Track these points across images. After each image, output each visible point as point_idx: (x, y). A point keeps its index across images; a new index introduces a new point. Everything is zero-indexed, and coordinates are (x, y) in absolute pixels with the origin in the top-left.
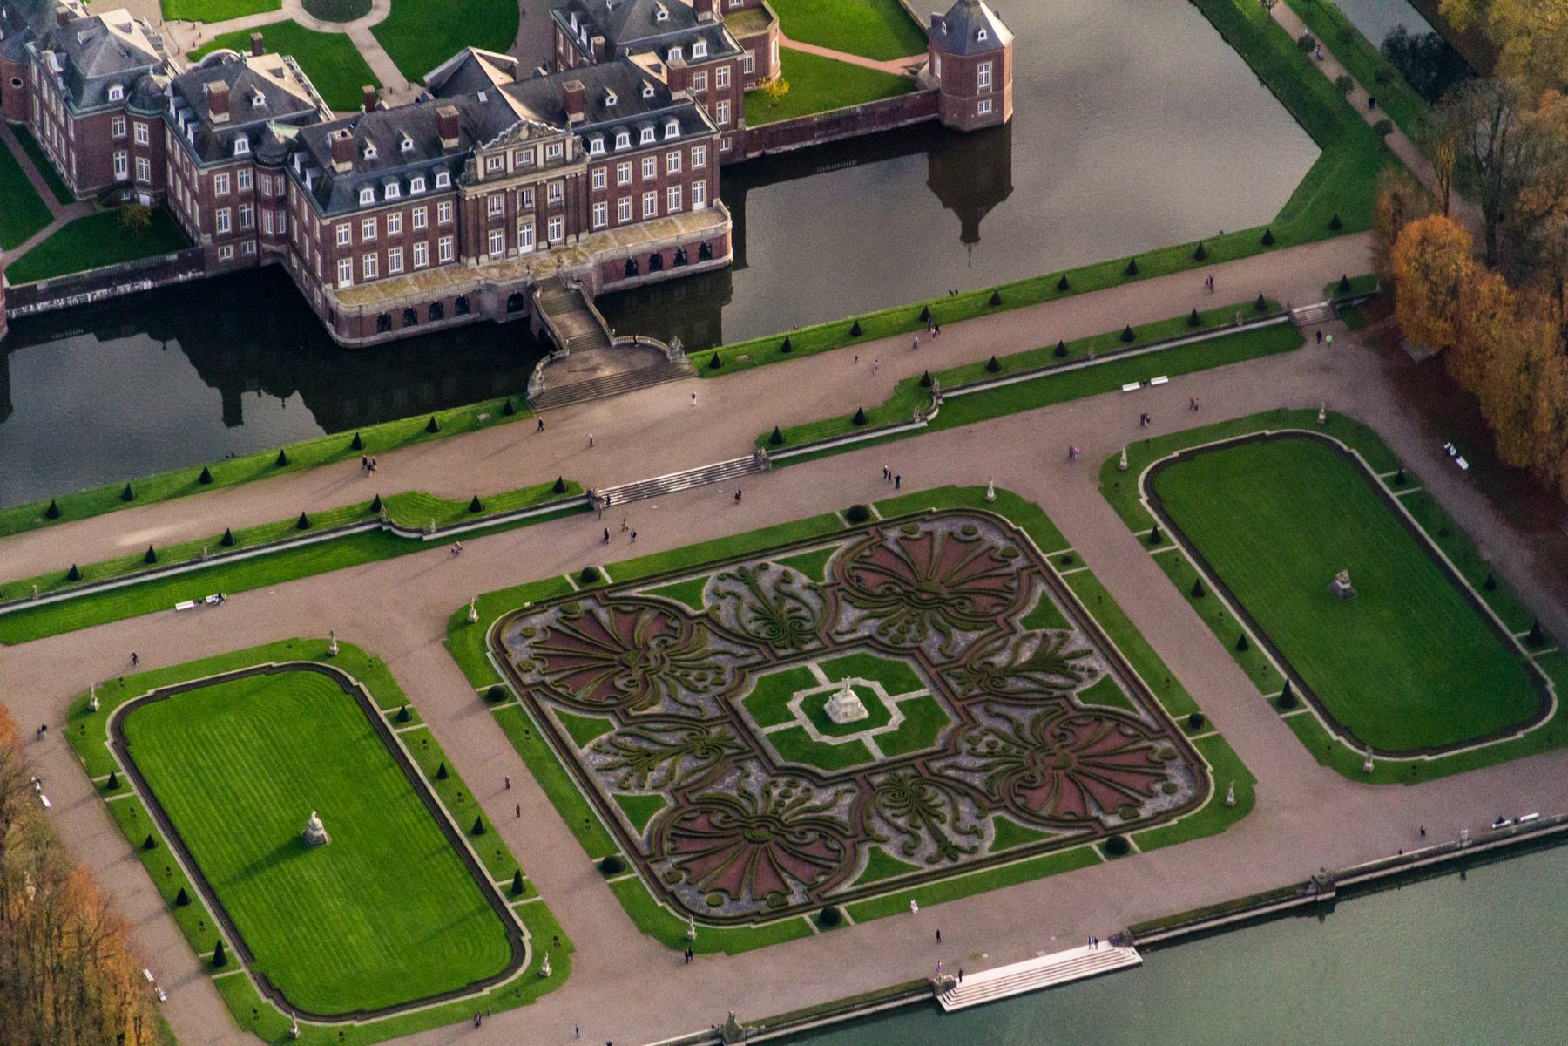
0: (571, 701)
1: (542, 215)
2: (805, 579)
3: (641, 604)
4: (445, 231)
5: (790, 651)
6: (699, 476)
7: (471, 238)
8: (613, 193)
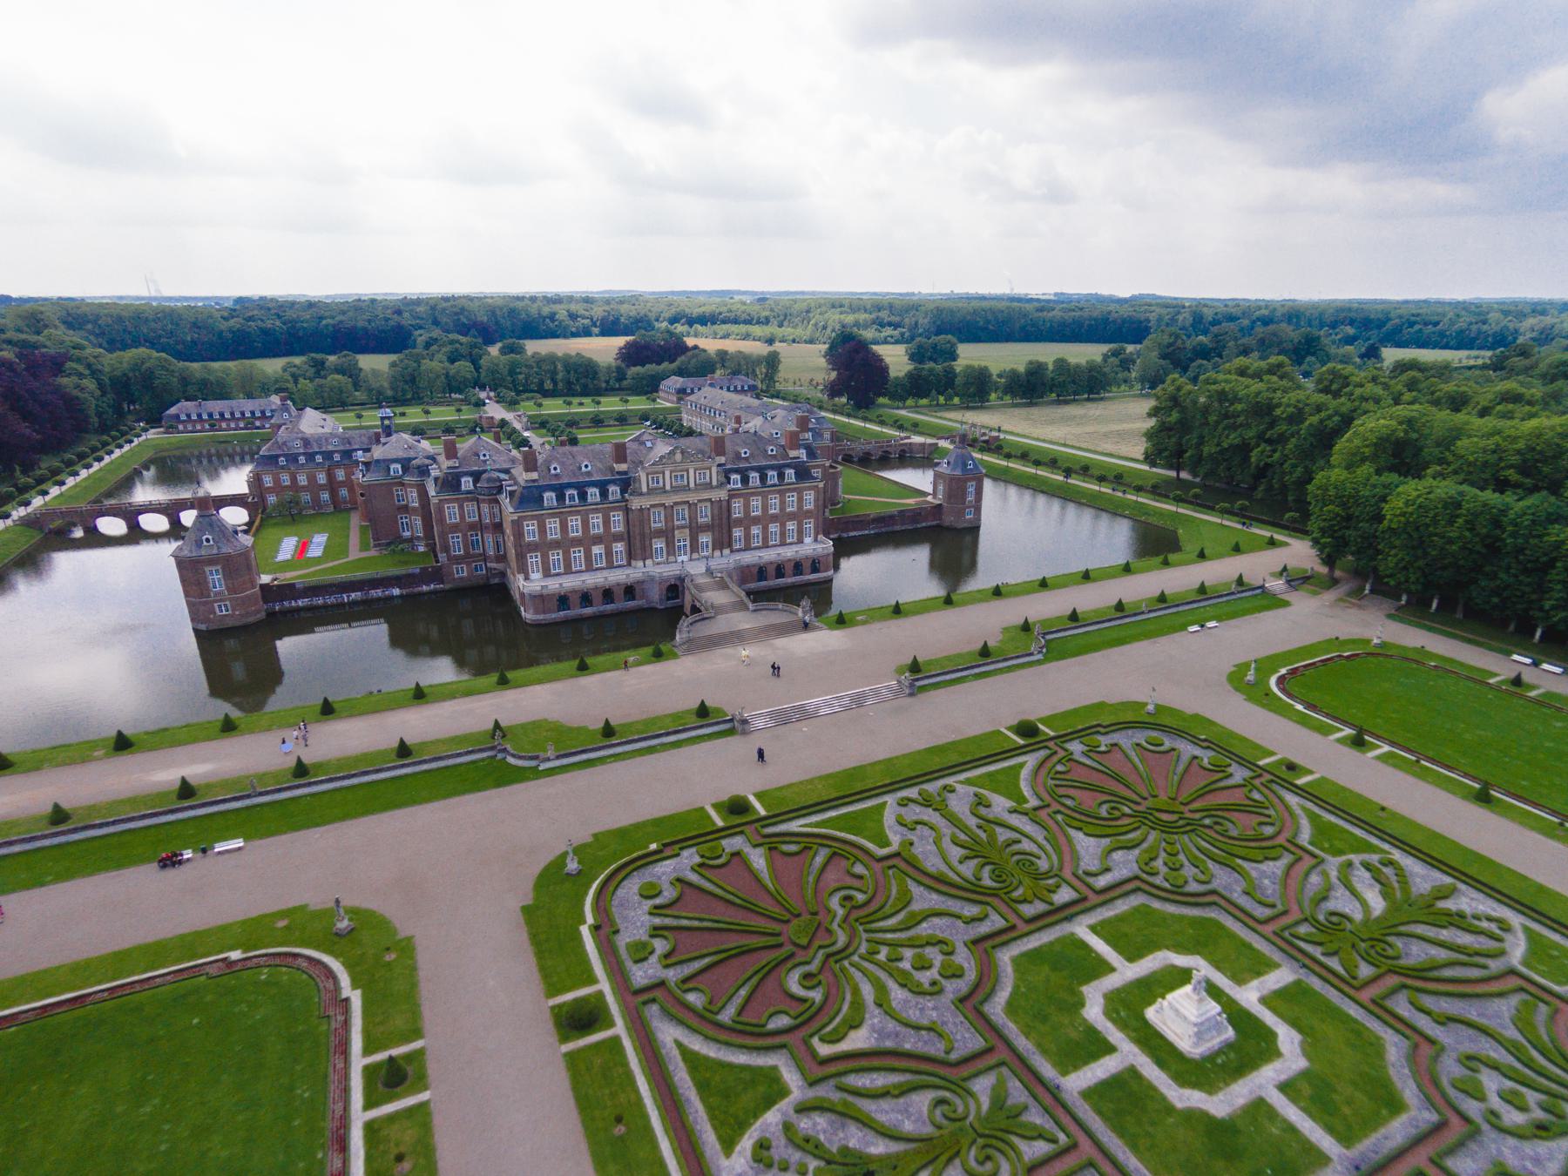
0: (703, 1022)
1: (695, 530)
2: (1010, 804)
3: (809, 842)
4: (617, 538)
5: (1040, 907)
6: (846, 701)
7: (638, 544)
8: (748, 521)
